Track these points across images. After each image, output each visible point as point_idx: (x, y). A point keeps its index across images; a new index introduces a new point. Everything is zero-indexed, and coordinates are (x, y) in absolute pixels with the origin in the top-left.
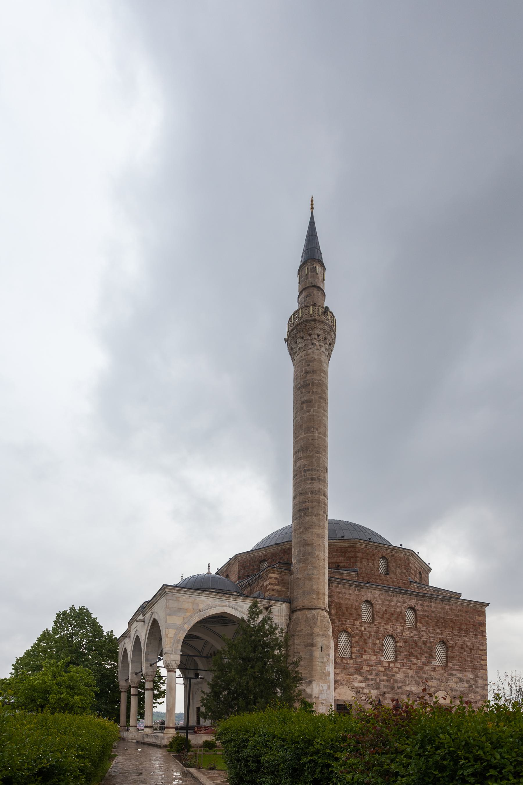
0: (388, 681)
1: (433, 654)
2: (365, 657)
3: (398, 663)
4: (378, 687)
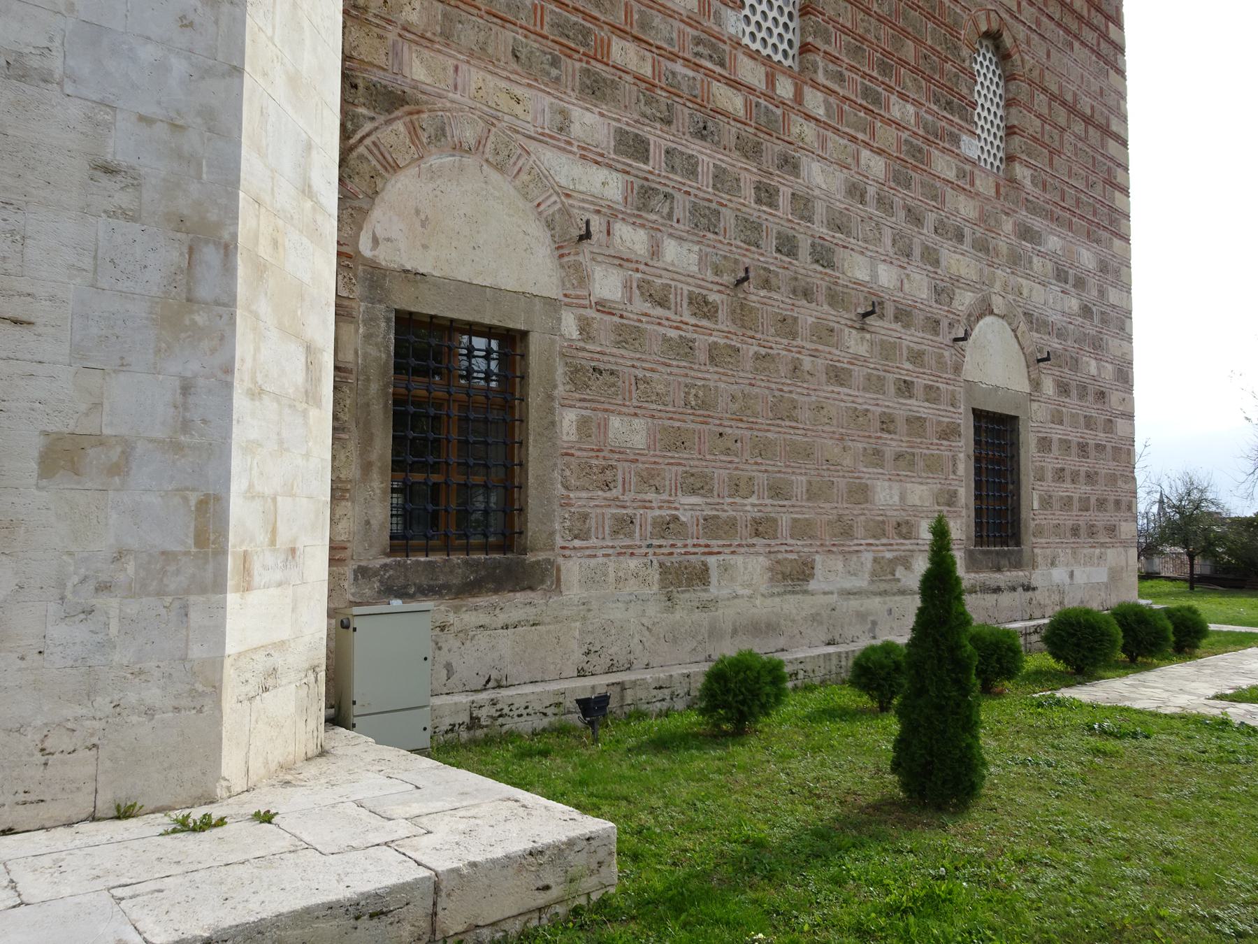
0: (766, 195)
1: (965, 91)
3: (815, 85)
4: (705, 220)
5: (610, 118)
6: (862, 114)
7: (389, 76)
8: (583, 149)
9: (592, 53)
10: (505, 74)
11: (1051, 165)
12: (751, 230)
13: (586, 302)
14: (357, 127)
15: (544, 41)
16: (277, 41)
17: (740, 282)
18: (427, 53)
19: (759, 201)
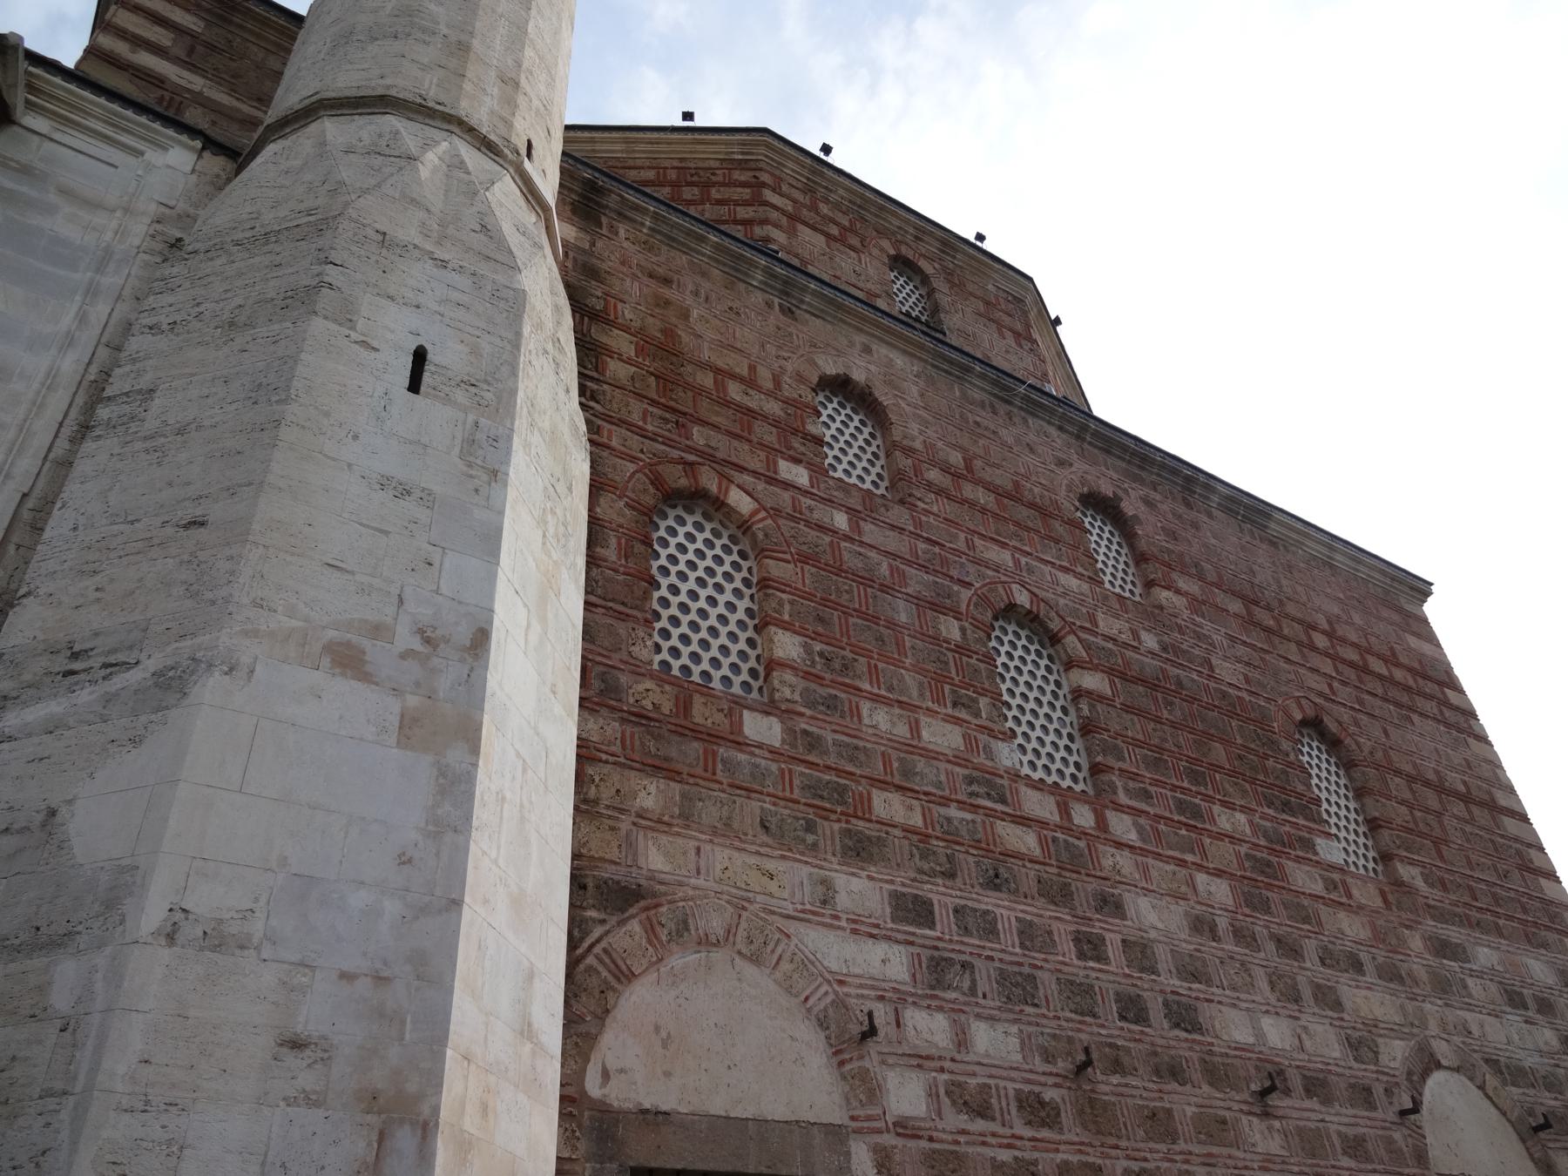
0: (1090, 947)
1: (1300, 788)
2: (880, 719)
3: (1119, 808)
4: (1018, 990)
5: (881, 880)
6: (1183, 832)
7: (623, 870)
8: (854, 921)
9: (851, 811)
10: (754, 848)
11: (1442, 858)
12: (1081, 995)
13: (880, 1124)
14: (587, 933)
15: (796, 806)
16: (501, 862)
17: (1081, 1068)
18: (664, 839)
19: (1081, 955)
